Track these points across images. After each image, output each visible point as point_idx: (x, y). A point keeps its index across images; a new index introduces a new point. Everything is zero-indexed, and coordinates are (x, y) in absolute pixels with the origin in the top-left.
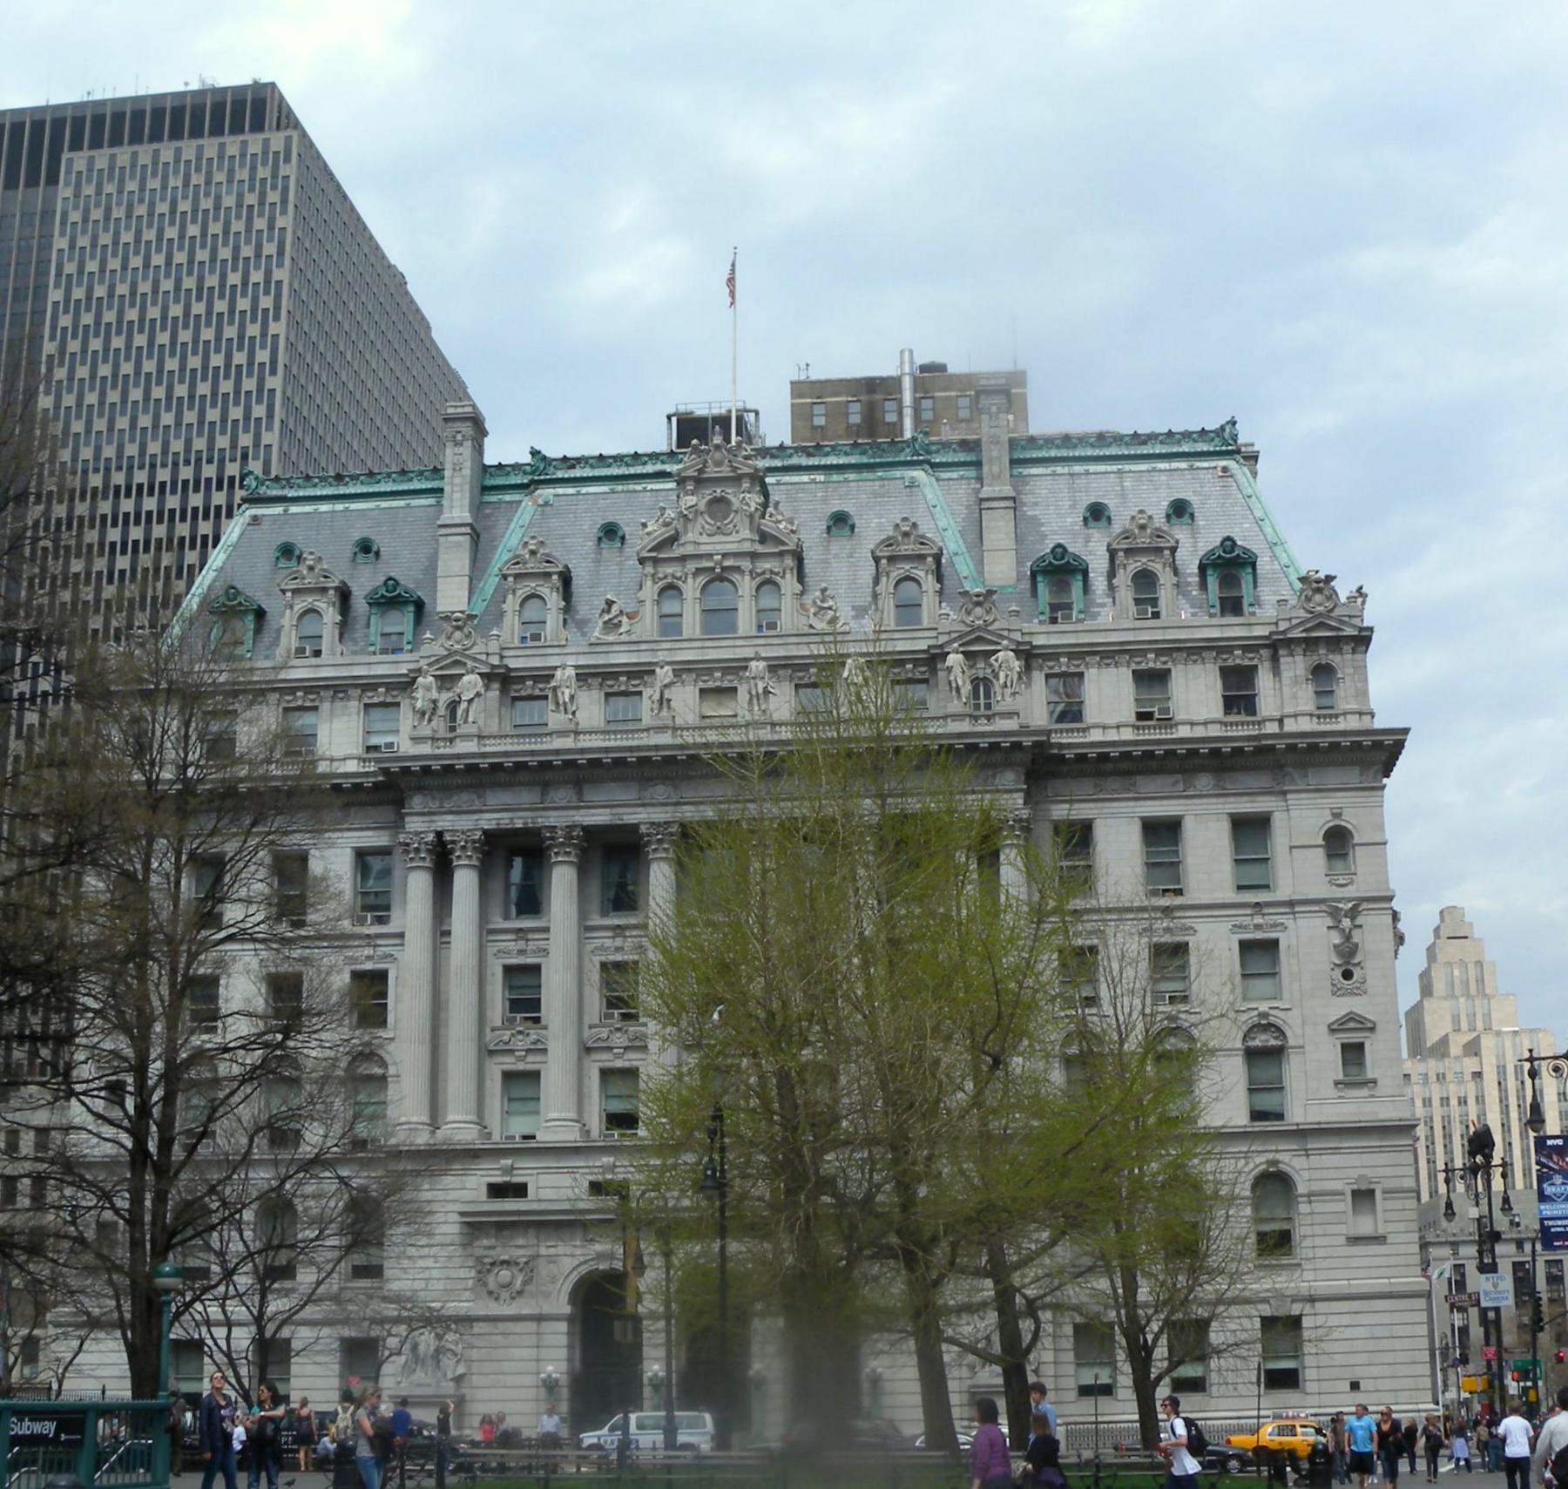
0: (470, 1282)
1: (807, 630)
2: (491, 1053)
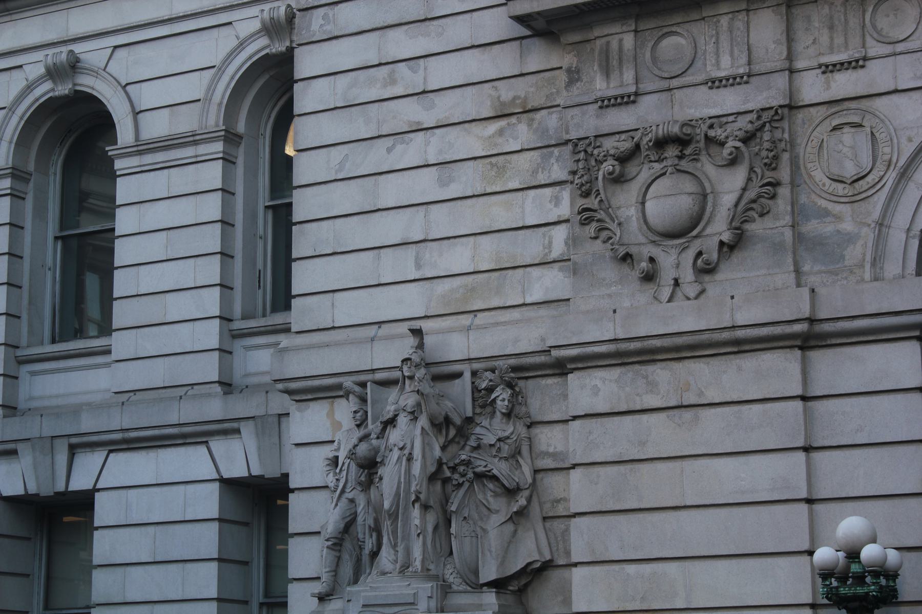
0: (560, 234)
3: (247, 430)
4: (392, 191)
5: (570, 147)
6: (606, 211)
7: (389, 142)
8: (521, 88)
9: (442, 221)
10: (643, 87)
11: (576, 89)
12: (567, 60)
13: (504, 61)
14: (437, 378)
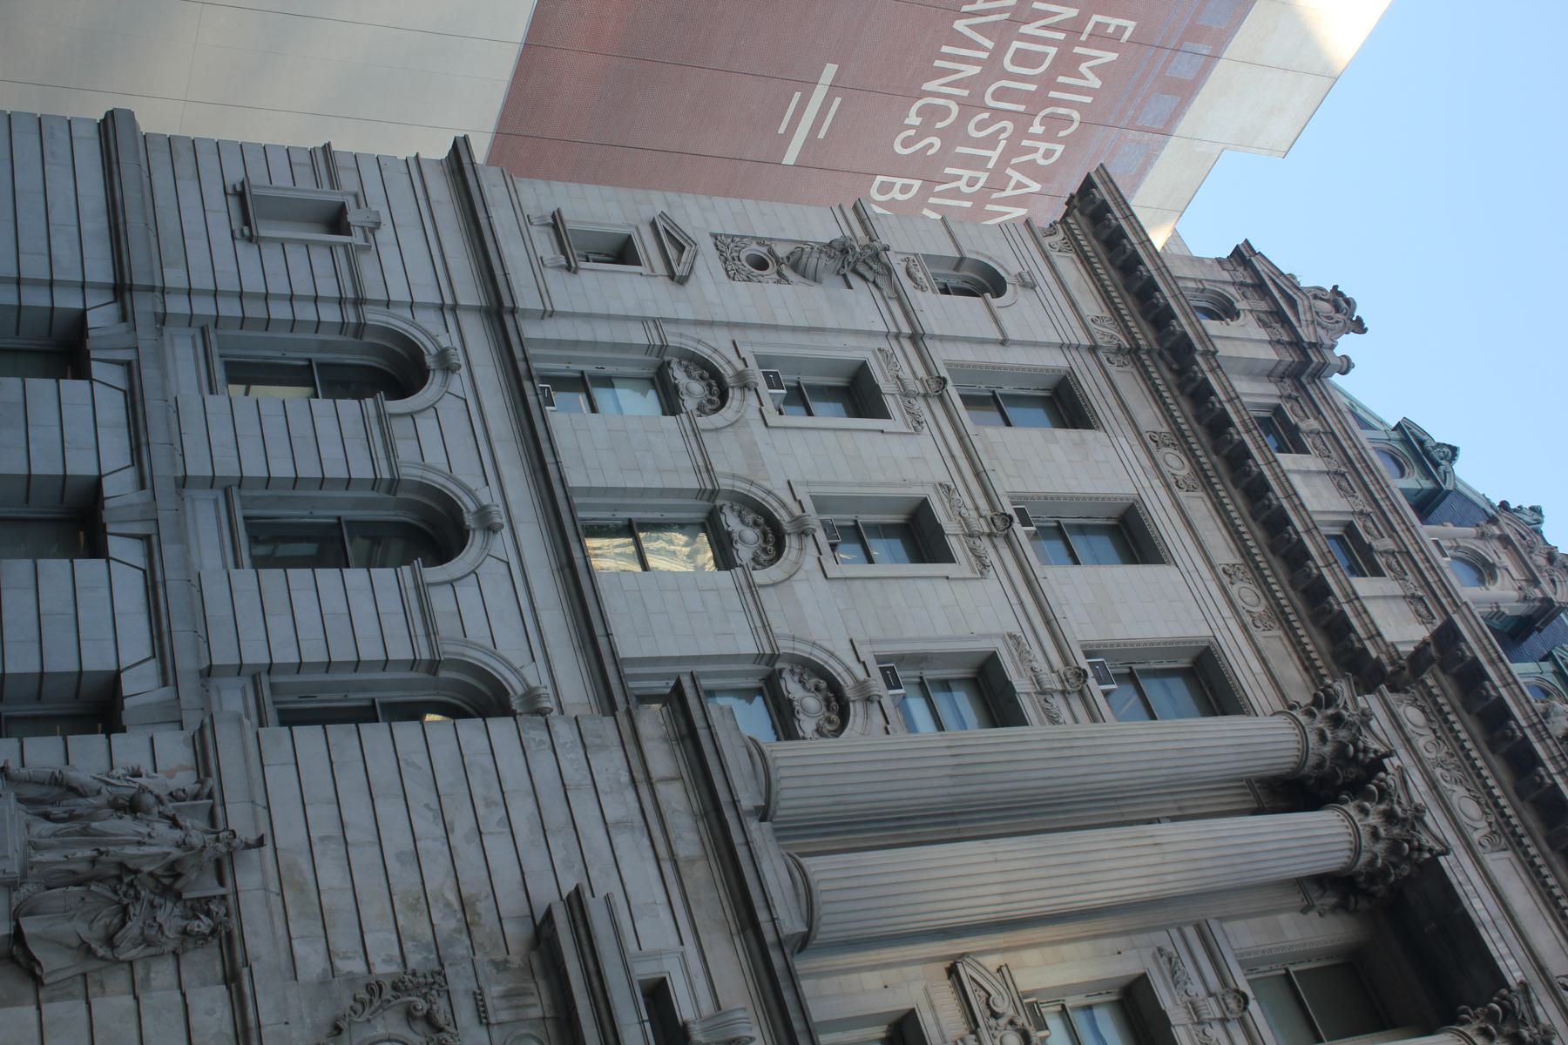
0: (358, 966)
2: (952, 972)
3: (167, 693)
4: (390, 810)
5: (438, 968)
6: (381, 1007)
7: (435, 805)
8: (489, 919)
9: (365, 857)
10: (495, 1031)
11: (489, 969)
12: (516, 960)
13: (511, 902)
14: (218, 863)
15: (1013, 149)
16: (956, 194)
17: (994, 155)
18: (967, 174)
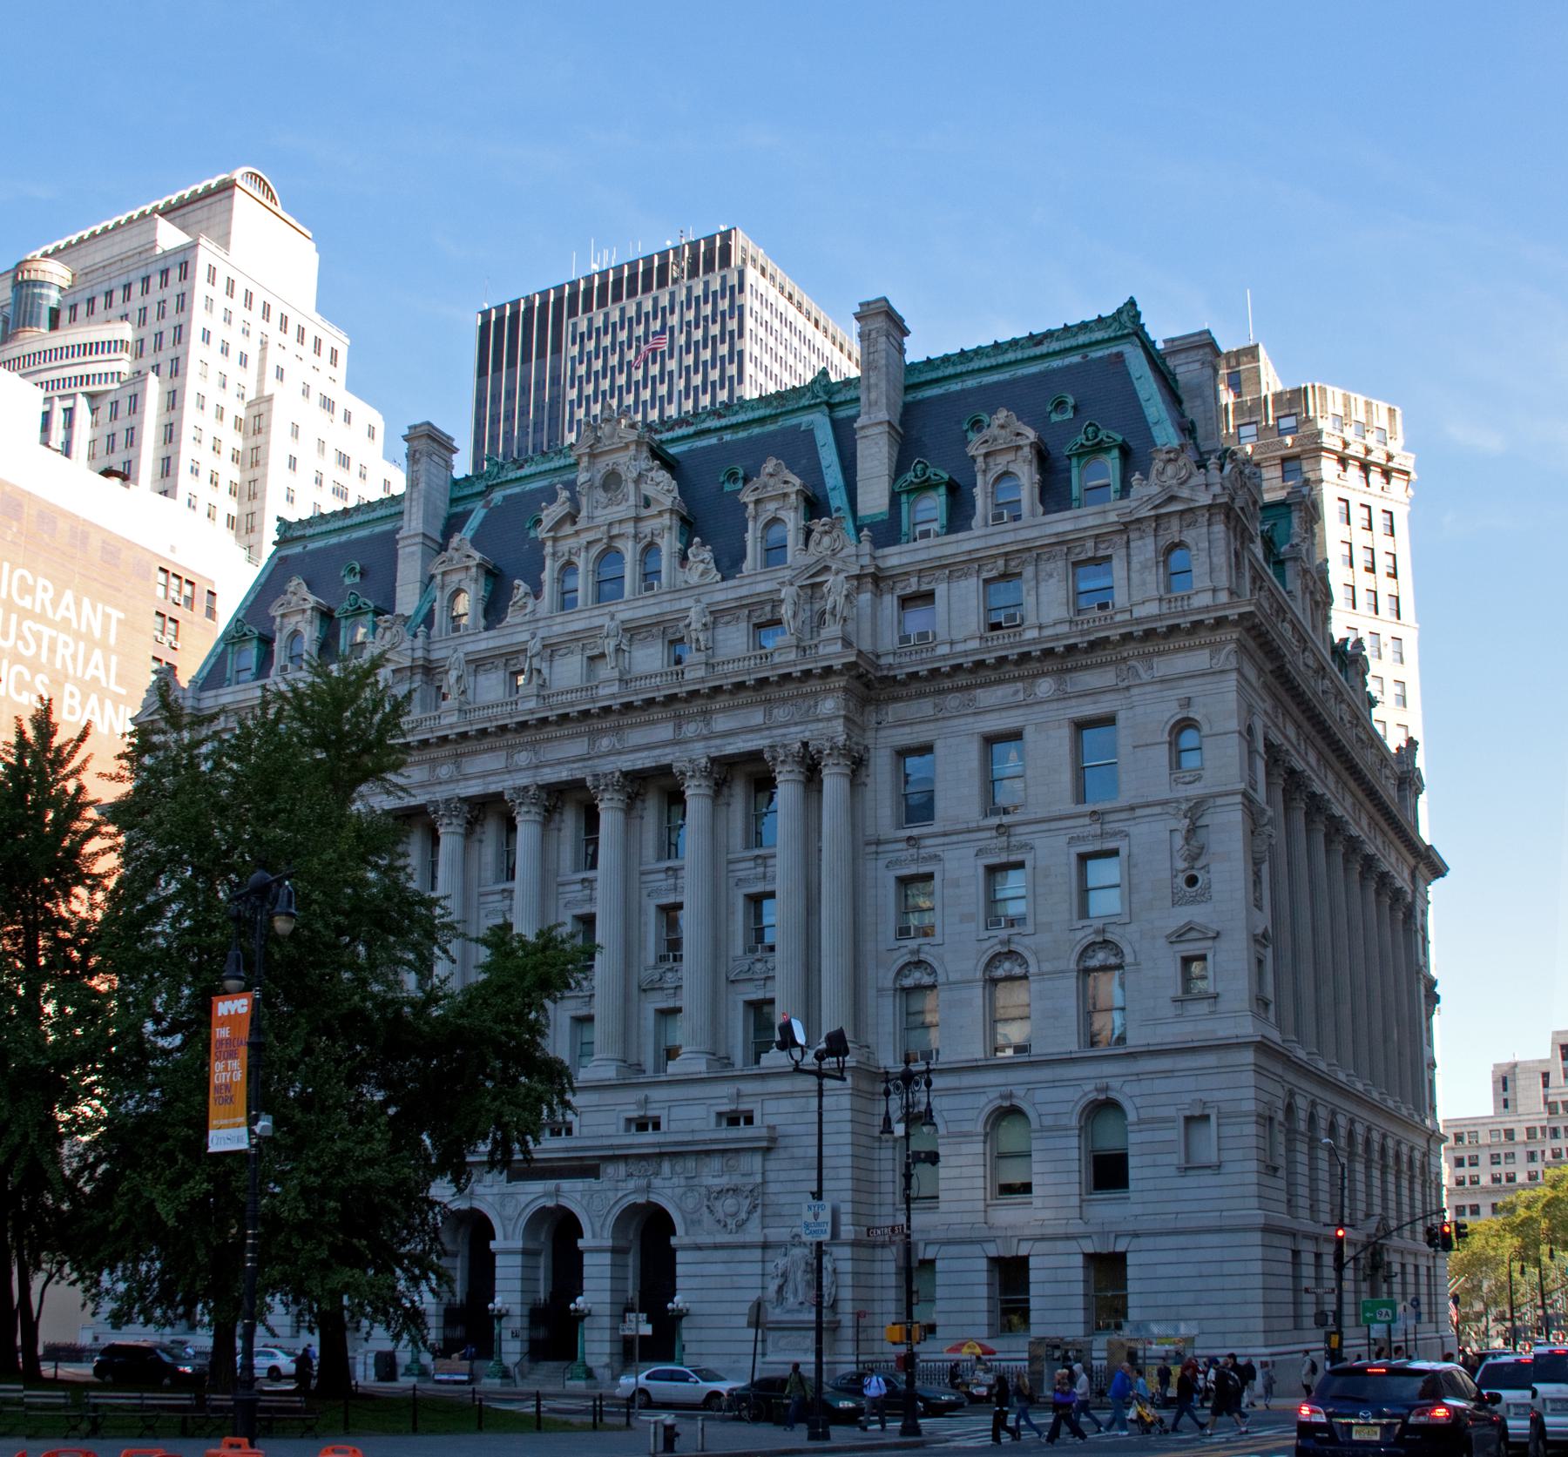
1: (684, 586)
15: (41, 618)
16: (74, 658)
17: (47, 632)
18: (60, 650)
